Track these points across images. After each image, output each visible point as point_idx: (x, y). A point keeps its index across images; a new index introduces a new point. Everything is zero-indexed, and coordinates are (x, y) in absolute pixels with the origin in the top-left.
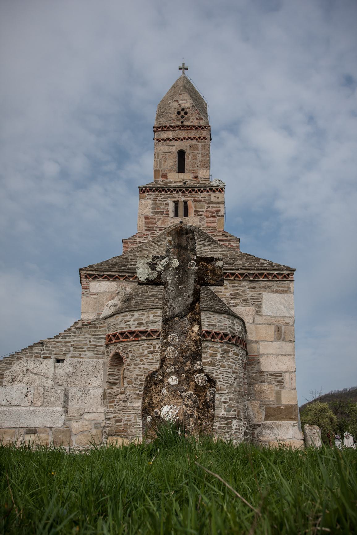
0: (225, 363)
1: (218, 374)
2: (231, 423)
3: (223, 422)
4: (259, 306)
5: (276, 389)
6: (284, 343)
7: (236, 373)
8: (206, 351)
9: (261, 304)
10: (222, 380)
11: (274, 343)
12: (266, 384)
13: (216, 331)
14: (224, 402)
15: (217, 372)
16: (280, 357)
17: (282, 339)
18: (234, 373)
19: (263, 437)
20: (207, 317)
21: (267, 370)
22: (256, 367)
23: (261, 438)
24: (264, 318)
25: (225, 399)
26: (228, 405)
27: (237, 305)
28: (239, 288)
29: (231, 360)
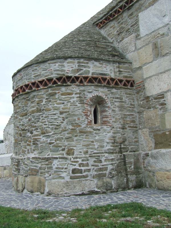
0: (50, 106)
1: (43, 118)
2: (51, 163)
3: (43, 163)
4: (138, 30)
5: (160, 113)
6: (162, 59)
7: (65, 112)
8: (35, 100)
9: (139, 27)
10: (47, 123)
11: (155, 62)
12: (152, 109)
13: (40, 79)
14: (50, 143)
15: (42, 117)
16: (160, 76)
17: (159, 55)
18: (61, 113)
19: (151, 167)
20: (33, 71)
21: (151, 94)
22: (143, 93)
23: (149, 168)
24: (142, 39)
25: (50, 140)
26: (53, 146)
27: (123, 39)
28: (122, 21)
29: (58, 101)
